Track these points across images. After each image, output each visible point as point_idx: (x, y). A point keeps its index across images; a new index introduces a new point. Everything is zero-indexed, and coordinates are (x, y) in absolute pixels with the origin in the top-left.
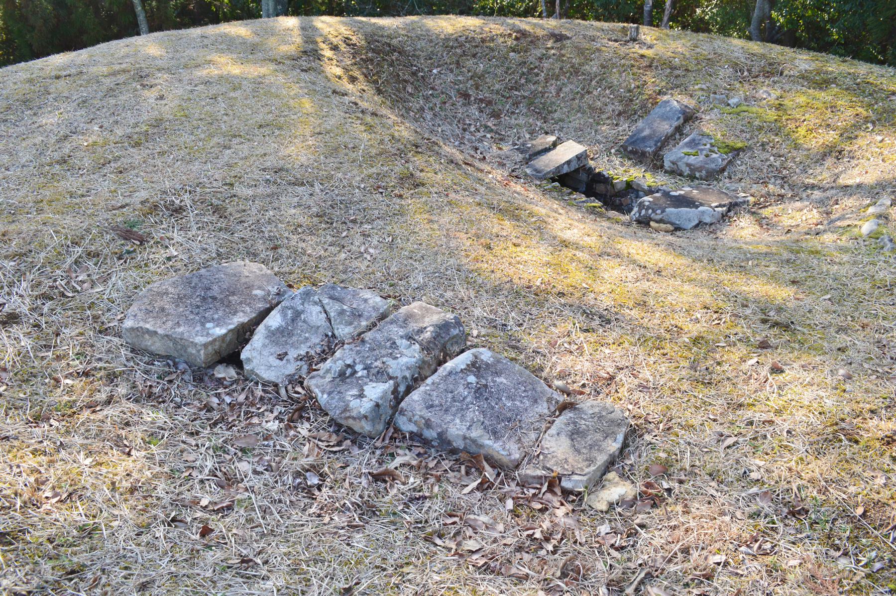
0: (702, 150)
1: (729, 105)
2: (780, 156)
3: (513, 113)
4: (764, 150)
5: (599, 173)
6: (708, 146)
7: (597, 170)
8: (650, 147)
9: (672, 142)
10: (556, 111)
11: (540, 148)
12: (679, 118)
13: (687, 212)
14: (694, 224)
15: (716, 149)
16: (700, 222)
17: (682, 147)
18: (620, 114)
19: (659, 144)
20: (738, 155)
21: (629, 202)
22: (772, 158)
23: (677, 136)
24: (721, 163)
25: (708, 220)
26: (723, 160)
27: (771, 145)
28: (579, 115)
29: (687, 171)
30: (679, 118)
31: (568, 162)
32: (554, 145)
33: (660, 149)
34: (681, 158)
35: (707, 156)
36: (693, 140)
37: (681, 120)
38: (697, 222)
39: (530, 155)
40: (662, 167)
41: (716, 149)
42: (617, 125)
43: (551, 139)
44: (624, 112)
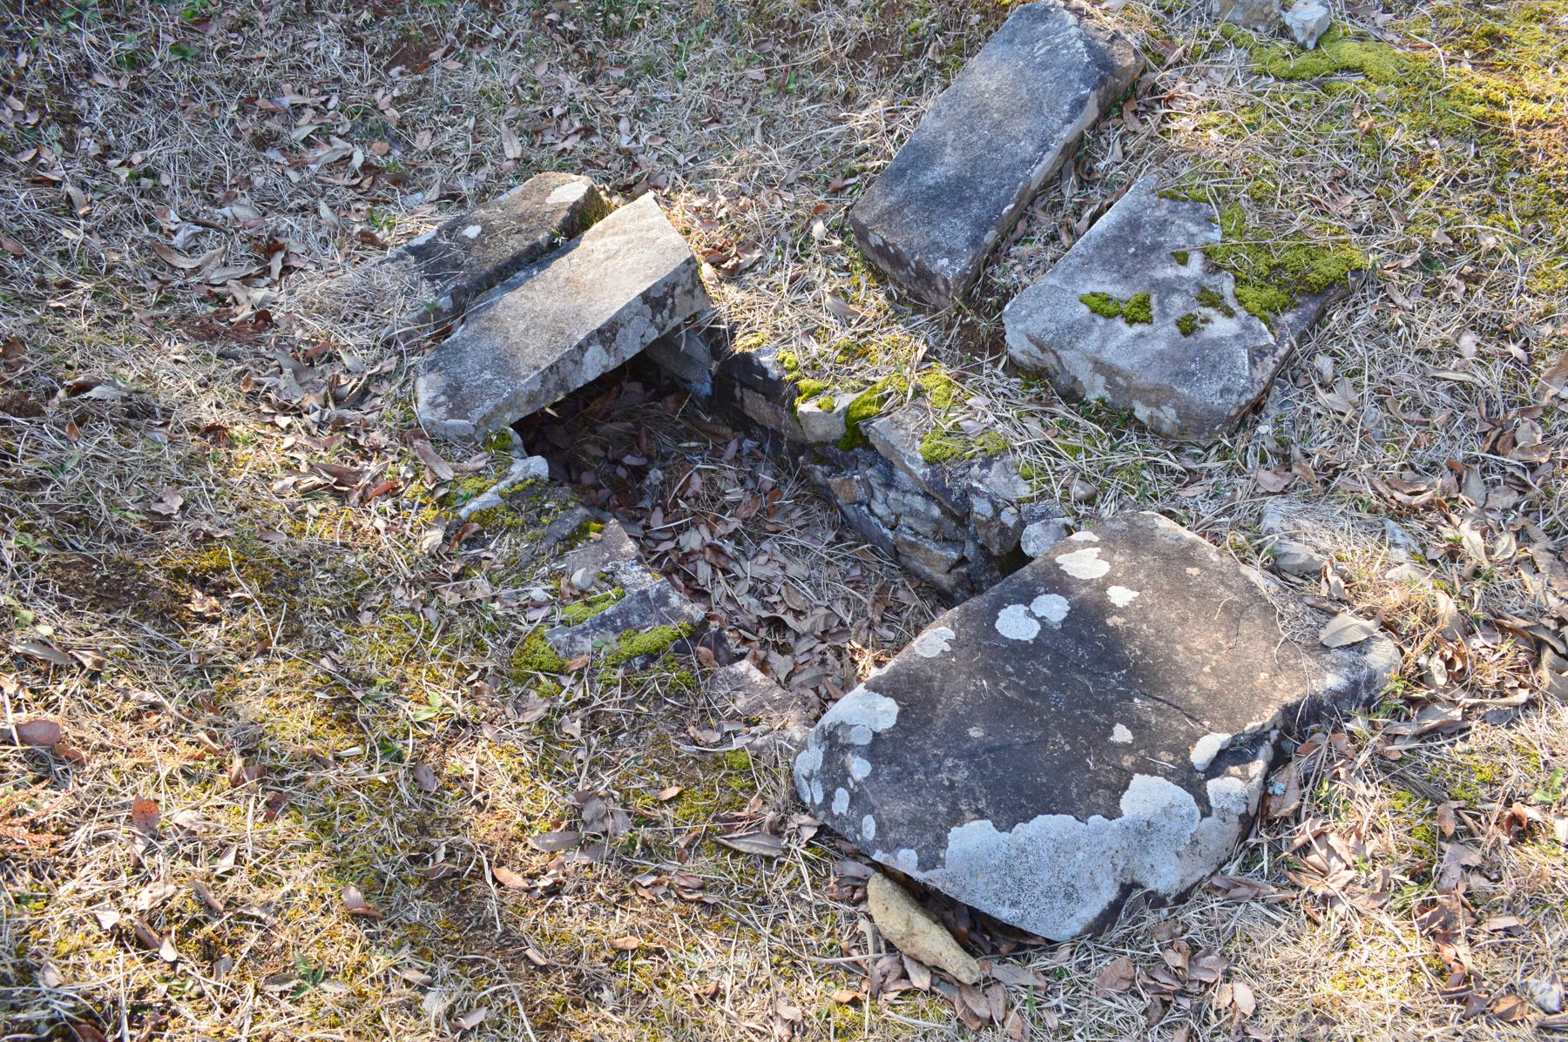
0: (1168, 288)
1: (1284, 31)
2: (1504, 335)
3: (476, 41)
4: (1434, 289)
5: (746, 358)
6: (1195, 266)
7: (741, 344)
8: (950, 253)
9: (1046, 222)
10: (635, 26)
11: (515, 245)
12: (1080, 104)
13: (1061, 848)
14: (1090, 910)
15: (1227, 286)
16: (1126, 889)
17: (1086, 264)
18: (861, 51)
19: (990, 237)
20: (1321, 317)
21: (861, 493)
22: (1468, 342)
23: (1069, 188)
24: (1246, 376)
25: (1165, 876)
26: (1257, 355)
27: (1464, 263)
28: (718, 45)
29: (1096, 390)
30: (1080, 104)
31: (607, 334)
32: (580, 219)
33: (996, 254)
34: (1075, 330)
35: (1188, 327)
36: (1133, 224)
37: (1091, 112)
38: (1109, 894)
39: (457, 294)
40: (997, 343)
41: (1227, 286)
42: (848, 99)
43: (571, 189)
44: (879, 42)
